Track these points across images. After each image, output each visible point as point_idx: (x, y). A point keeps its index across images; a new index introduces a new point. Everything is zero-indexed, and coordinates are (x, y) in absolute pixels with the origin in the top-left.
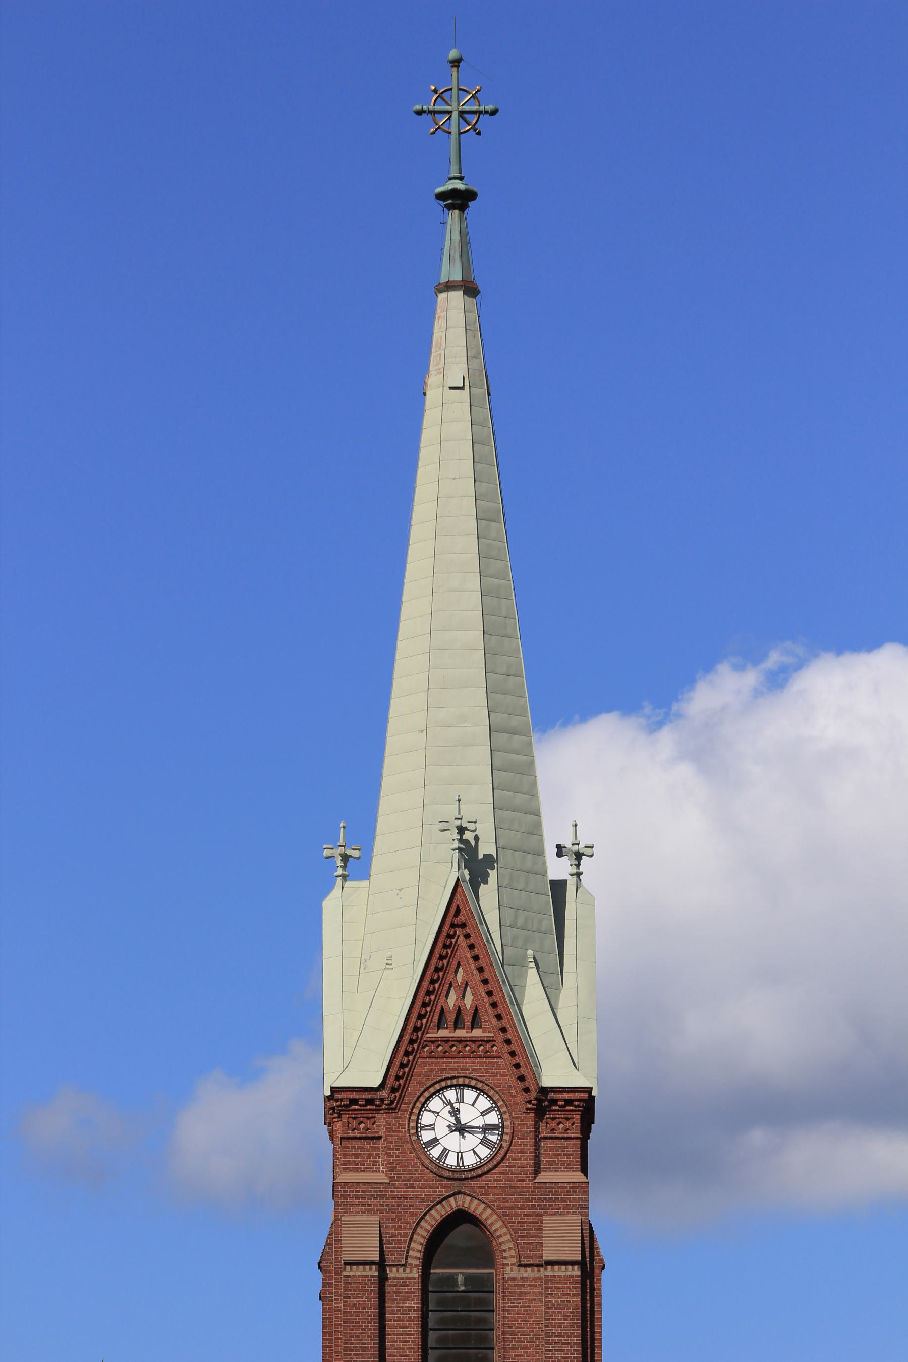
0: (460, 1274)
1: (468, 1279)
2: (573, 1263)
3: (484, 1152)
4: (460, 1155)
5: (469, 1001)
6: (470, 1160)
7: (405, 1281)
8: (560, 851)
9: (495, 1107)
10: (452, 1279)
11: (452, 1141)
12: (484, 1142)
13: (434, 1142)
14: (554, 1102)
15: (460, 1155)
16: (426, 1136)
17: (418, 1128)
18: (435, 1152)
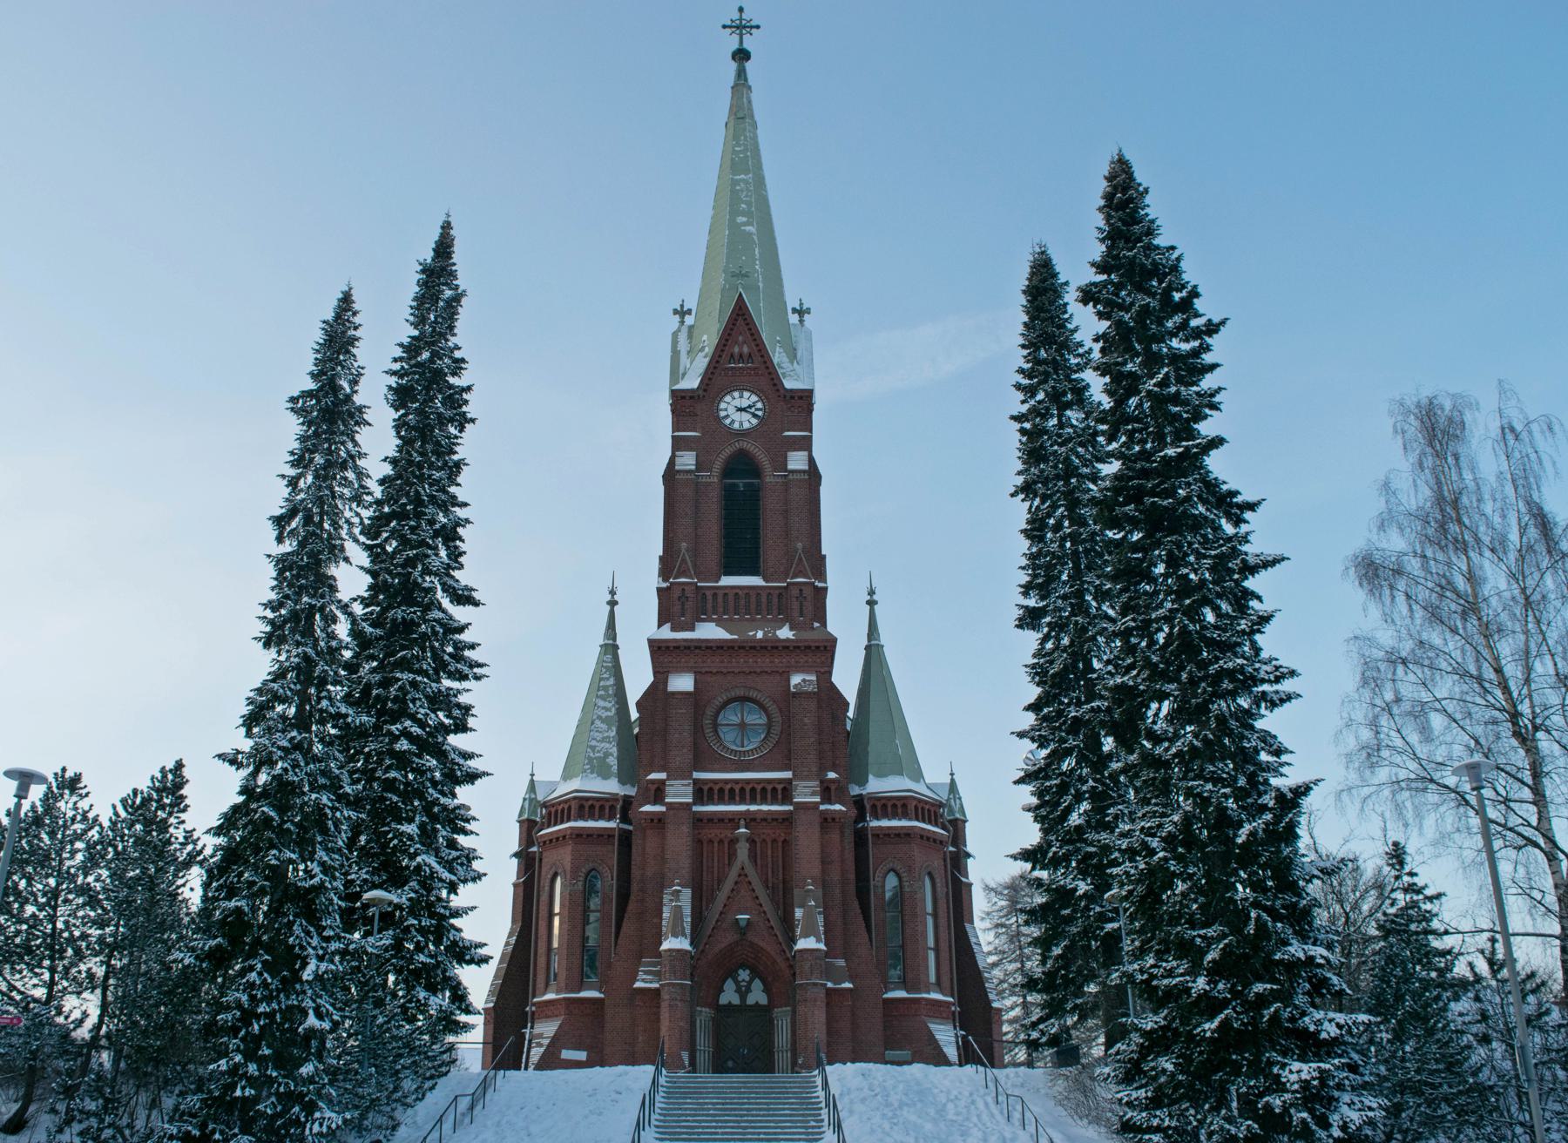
0: (741, 483)
1: (745, 485)
2: (804, 472)
3: (754, 421)
4: (741, 424)
5: (746, 350)
6: (746, 425)
7: (709, 484)
8: (794, 310)
9: (764, 409)
10: (735, 485)
11: (737, 416)
12: (755, 416)
13: (727, 416)
14: (792, 398)
15: (741, 424)
16: (723, 414)
17: (718, 410)
18: (727, 422)
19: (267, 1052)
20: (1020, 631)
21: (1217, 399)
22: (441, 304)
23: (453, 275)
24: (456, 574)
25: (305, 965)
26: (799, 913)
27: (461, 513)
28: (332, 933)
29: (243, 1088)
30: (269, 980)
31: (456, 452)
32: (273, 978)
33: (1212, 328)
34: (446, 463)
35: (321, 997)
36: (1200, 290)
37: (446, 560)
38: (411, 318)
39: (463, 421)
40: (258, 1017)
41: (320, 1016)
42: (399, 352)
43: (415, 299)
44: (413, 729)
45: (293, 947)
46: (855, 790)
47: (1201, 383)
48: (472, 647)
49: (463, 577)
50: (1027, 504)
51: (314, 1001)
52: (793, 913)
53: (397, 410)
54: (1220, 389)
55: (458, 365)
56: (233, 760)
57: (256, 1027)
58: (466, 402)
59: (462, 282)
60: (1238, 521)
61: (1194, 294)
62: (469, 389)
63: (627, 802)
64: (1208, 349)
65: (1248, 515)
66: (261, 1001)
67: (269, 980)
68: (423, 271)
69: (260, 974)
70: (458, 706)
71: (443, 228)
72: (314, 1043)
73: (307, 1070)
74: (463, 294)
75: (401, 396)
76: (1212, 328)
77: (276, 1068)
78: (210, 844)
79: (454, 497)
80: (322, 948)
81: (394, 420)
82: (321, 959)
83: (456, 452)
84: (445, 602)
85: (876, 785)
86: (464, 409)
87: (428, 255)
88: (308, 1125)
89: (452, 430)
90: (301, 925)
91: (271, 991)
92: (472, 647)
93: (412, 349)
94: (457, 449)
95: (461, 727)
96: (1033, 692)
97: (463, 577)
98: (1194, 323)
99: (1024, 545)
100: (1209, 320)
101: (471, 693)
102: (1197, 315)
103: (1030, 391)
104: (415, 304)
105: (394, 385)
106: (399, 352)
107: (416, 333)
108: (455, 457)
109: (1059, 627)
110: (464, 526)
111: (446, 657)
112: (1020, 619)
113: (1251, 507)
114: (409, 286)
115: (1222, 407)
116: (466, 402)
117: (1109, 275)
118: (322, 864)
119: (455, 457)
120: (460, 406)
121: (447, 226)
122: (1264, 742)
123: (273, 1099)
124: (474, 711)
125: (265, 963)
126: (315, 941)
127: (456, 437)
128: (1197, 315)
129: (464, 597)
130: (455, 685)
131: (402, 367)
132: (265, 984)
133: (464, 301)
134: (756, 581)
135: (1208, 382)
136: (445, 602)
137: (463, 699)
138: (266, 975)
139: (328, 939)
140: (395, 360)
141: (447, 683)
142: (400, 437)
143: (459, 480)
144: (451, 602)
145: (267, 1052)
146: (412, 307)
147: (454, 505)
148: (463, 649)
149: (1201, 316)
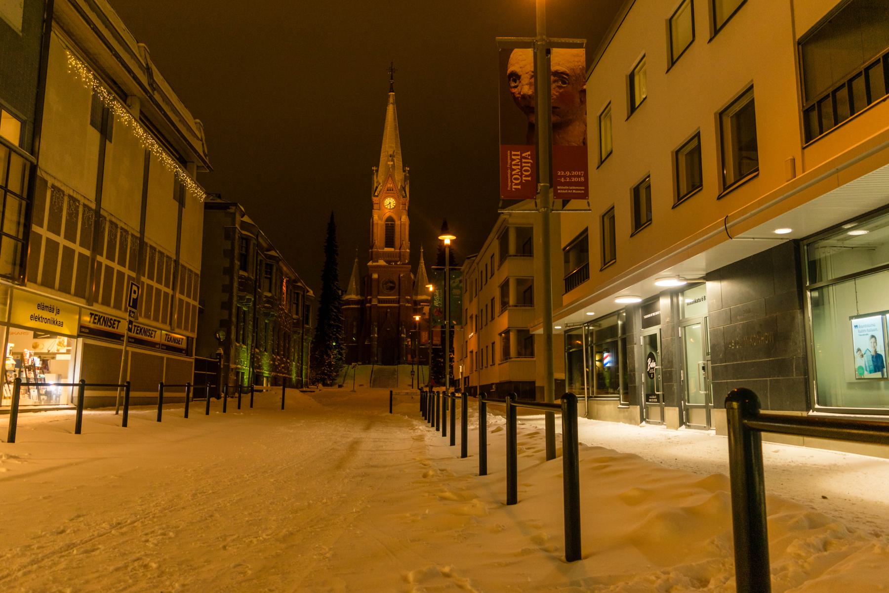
26: (400, 328)
46: (414, 298)
63: (363, 300)
85: (420, 298)
134: (392, 250)
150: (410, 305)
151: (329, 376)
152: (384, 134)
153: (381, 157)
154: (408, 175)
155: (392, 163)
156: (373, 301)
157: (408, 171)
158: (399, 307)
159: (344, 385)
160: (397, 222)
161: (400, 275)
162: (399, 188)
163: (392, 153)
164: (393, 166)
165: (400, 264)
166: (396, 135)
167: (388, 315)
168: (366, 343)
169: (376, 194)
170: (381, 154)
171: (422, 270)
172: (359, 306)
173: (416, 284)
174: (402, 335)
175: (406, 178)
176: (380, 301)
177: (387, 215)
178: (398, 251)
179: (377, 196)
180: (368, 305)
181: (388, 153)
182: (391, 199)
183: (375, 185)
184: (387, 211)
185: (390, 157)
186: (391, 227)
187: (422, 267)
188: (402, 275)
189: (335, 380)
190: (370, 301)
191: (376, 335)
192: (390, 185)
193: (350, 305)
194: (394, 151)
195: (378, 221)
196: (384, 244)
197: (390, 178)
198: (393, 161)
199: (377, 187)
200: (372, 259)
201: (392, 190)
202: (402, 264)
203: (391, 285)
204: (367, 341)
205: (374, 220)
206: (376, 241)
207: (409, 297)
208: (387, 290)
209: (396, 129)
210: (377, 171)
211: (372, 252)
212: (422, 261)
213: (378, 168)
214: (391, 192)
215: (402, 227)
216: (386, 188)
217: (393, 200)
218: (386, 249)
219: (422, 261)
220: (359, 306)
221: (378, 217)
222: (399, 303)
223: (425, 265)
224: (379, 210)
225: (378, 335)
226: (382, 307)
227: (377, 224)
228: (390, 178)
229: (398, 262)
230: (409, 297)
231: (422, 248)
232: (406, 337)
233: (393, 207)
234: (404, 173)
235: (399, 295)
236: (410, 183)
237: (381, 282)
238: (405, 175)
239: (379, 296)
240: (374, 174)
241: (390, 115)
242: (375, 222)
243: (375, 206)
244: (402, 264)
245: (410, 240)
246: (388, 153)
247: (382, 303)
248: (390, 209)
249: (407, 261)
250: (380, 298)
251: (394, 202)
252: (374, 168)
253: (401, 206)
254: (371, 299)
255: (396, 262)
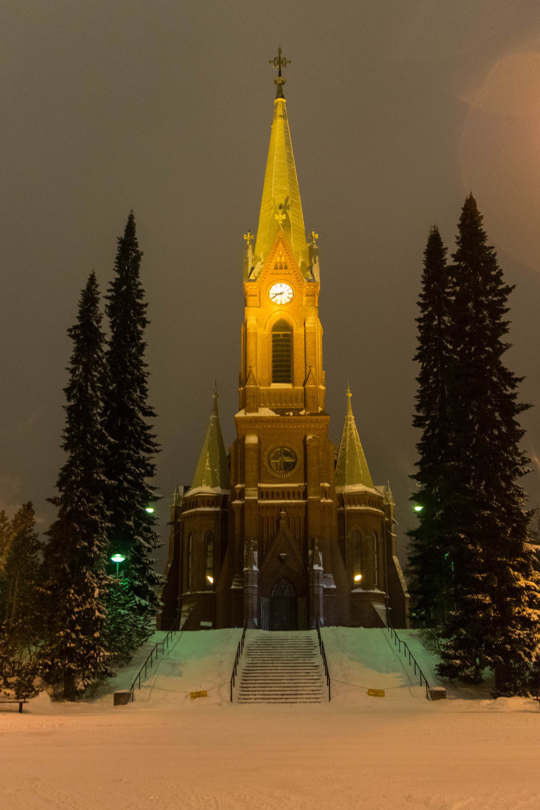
19: (79, 628)
20: (414, 428)
21: (507, 327)
22: (130, 260)
23: (136, 245)
24: (145, 400)
25: (93, 591)
27: (144, 369)
28: (102, 577)
29: (70, 644)
30: (78, 598)
31: (141, 339)
32: (79, 596)
33: (508, 290)
34: (137, 345)
35: (99, 604)
36: (503, 272)
37: (139, 393)
38: (116, 269)
39: (144, 323)
40: (74, 613)
41: (100, 612)
42: (111, 287)
43: (117, 258)
44: (128, 477)
45: (87, 583)
47: (501, 319)
48: (154, 436)
49: (148, 402)
50: (421, 364)
51: (97, 606)
52: (308, 552)
53: (111, 318)
54: (509, 322)
55: (140, 294)
56: (53, 501)
57: (74, 618)
58: (145, 313)
59: (140, 249)
60: (513, 387)
61: (500, 273)
62: (146, 305)
64: (505, 300)
65: (517, 384)
66: (75, 606)
67: (78, 598)
68: (120, 243)
69: (73, 595)
70: (149, 465)
71: (129, 218)
72: (99, 623)
73: (97, 635)
74: (142, 254)
75: (112, 311)
76: (508, 290)
77: (83, 634)
78: (45, 540)
79: (142, 362)
80: (99, 583)
81: (110, 322)
82: (99, 588)
83: (141, 339)
84: (140, 415)
86: (144, 316)
87: (122, 234)
88: (98, 658)
89: (140, 328)
90: (89, 573)
91: (79, 603)
92: (154, 436)
93: (117, 285)
94: (142, 337)
95: (150, 474)
96: (419, 458)
97: (148, 402)
98: (500, 287)
99: (418, 386)
100: (507, 286)
101: (155, 459)
102: (501, 283)
103: (424, 306)
104: (117, 261)
105: (109, 304)
106: (111, 287)
107: (118, 276)
108: (141, 341)
109: (432, 426)
110: (147, 377)
111: (142, 442)
112: (414, 422)
113: (520, 380)
114: (114, 251)
115: (509, 331)
116: (145, 313)
117: (460, 263)
118: (97, 546)
119: (141, 341)
120: (142, 314)
121: (131, 217)
122: (517, 491)
123: (82, 648)
124: (156, 467)
125: (74, 589)
126: (96, 580)
127: (141, 331)
128: (501, 283)
129: (148, 413)
130: (146, 455)
131: (113, 295)
132: (76, 599)
133: (142, 257)
135: (504, 318)
136: (140, 415)
137: (151, 462)
138: (76, 595)
139: (101, 579)
140: (109, 291)
141: (142, 454)
142: (113, 332)
143: (144, 353)
144: (143, 414)
145: (79, 628)
146: (116, 263)
147: (142, 365)
148: (149, 438)
149: (503, 284)
150: (330, 501)
151: (83, 661)
152: (267, 171)
153: (262, 212)
154: (315, 247)
155: (284, 217)
156: (247, 492)
157: (316, 239)
158: (306, 506)
159: (137, 693)
160: (298, 331)
161: (305, 440)
162: (300, 265)
163: (283, 202)
164: (287, 224)
165: (305, 415)
166: (291, 171)
167: (283, 522)
168: (233, 587)
169: (252, 277)
170: (262, 207)
171: (351, 434)
172: (218, 509)
173: (338, 464)
174: (316, 567)
175: (311, 253)
176: (263, 494)
177: (277, 316)
178: (302, 388)
179: (254, 281)
180: (236, 502)
181: (274, 202)
182: (284, 285)
183: (250, 265)
184: (276, 308)
185: (280, 208)
186: (282, 340)
187: (351, 429)
188: (310, 437)
189: (110, 675)
190: (241, 494)
191: (255, 568)
192: (280, 258)
193: (197, 506)
194: (288, 197)
195: (256, 328)
196: (271, 375)
197: (280, 244)
198: (284, 213)
199: (253, 269)
200: (243, 406)
201: (286, 268)
202: (310, 415)
203: (288, 460)
204: (234, 583)
205: (248, 326)
206: (254, 370)
207: (327, 485)
208: (281, 470)
209: (290, 162)
210: (253, 242)
211: (245, 390)
212: (351, 415)
213: (256, 237)
214: (283, 271)
215: (307, 338)
216: (272, 267)
217: (288, 287)
218: (276, 386)
219: (351, 415)
220: (218, 509)
221: (257, 320)
222: (305, 497)
223: (356, 423)
224: (259, 307)
225: (259, 567)
226: (268, 506)
227: (256, 334)
228: (280, 244)
229: (301, 410)
230: (327, 485)
231: (348, 390)
232: (324, 572)
233: (288, 300)
234: (309, 245)
235: (305, 481)
236: (320, 261)
237: (266, 454)
238: (311, 248)
239: (260, 483)
240: (248, 247)
241: (278, 128)
242: (251, 330)
243: (251, 301)
244: (310, 415)
245: (324, 367)
246: (274, 202)
247: (268, 498)
248: (281, 305)
249: (320, 409)
250: (263, 488)
251: (291, 291)
252: (247, 237)
253: (305, 299)
254: (242, 491)
255: (296, 411)
